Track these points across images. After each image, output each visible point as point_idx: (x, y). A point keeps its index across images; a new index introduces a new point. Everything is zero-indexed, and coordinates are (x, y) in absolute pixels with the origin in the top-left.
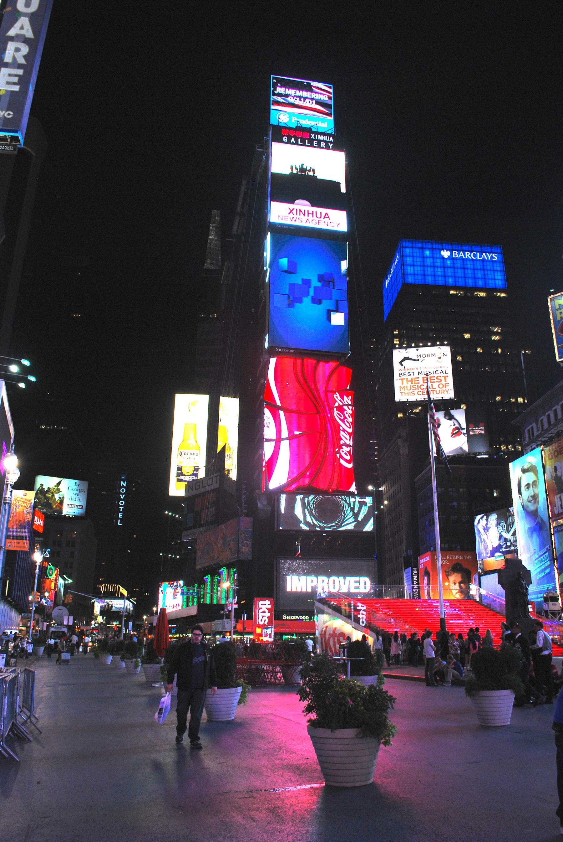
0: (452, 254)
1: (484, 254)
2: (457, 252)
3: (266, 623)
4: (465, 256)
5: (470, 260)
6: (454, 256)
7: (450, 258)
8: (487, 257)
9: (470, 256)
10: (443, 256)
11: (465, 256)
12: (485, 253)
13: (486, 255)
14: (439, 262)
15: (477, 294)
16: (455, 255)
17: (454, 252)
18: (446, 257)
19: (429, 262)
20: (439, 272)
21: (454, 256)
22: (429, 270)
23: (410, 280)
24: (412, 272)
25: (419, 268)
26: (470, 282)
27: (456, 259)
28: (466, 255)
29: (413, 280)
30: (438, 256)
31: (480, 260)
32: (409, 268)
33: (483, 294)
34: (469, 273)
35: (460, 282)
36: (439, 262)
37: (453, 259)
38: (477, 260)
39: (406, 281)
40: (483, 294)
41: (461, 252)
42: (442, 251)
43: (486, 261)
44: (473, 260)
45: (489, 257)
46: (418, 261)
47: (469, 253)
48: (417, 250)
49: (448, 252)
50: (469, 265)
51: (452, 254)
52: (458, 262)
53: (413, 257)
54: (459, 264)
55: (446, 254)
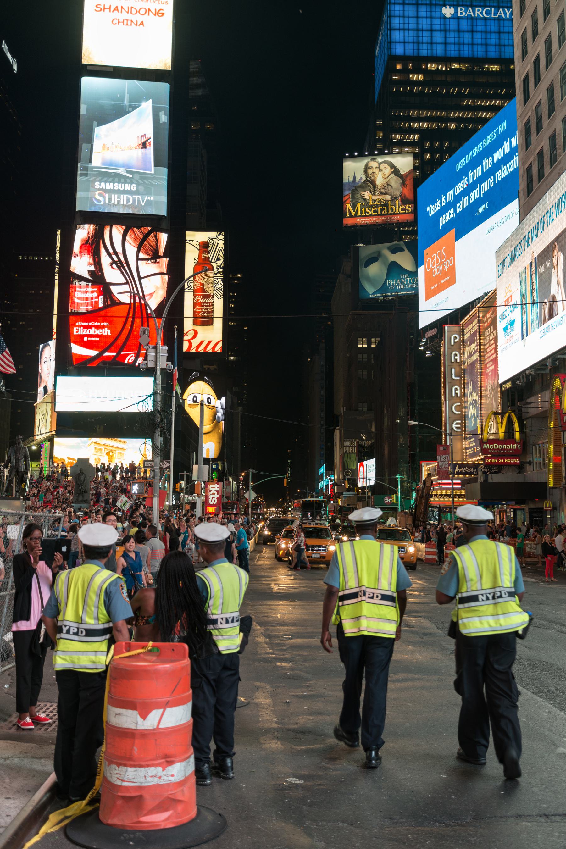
0: (456, 12)
1: (501, 10)
2: (463, 9)
3: (215, 503)
4: (474, 13)
5: (481, 19)
6: (459, 15)
7: (454, 17)
8: (505, 14)
9: (482, 13)
10: (444, 15)
11: (474, 13)
12: (503, 7)
13: (504, 11)
14: (438, 24)
15: (488, 68)
16: (461, 13)
17: (459, 8)
18: (448, 16)
19: (425, 23)
20: (438, 37)
21: (459, 15)
22: (424, 36)
23: (398, 50)
24: (402, 38)
25: (411, 33)
26: (479, 52)
27: (463, 18)
28: (477, 12)
29: (402, 51)
30: (438, 15)
31: (495, 19)
32: (397, 33)
33: (495, 68)
34: (479, 38)
35: (466, 52)
36: (438, 24)
37: (459, 18)
38: (490, 19)
39: (393, 51)
40: (495, 68)
41: (470, 9)
42: (444, 8)
43: (504, 19)
44: (485, 19)
45: (508, 13)
46: (411, 23)
47: (481, 10)
48: (411, 7)
49: (452, 9)
50: (480, 26)
51: (456, 12)
52: (465, 22)
53: (404, 17)
54: (465, 25)
55: (448, 11)
